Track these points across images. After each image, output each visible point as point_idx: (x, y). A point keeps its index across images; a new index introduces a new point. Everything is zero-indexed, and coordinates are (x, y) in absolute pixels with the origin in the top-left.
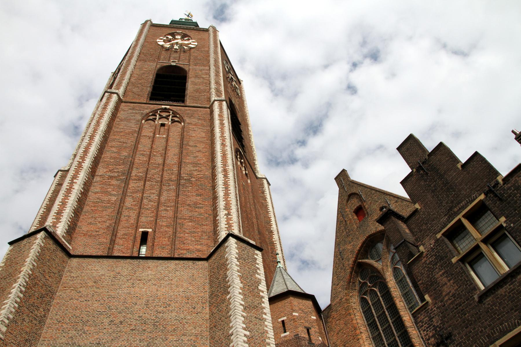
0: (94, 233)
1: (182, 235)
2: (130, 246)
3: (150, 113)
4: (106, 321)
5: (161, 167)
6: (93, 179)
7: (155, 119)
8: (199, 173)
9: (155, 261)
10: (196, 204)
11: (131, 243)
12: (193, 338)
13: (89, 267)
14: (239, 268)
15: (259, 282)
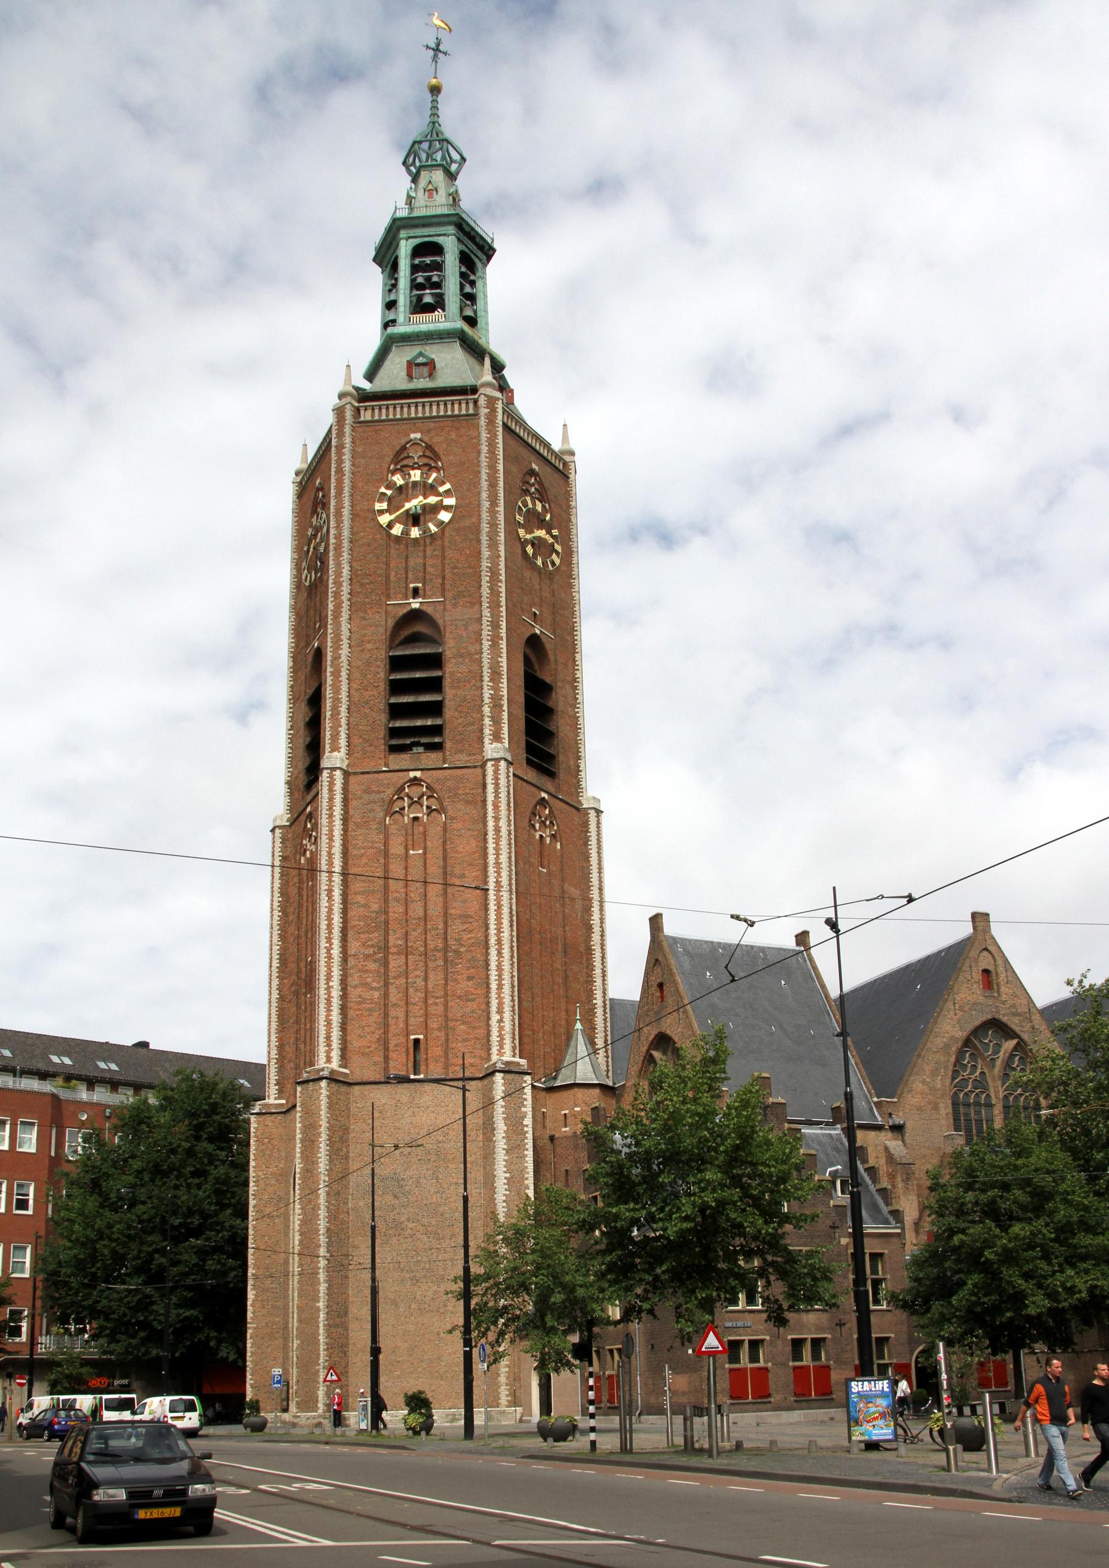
0: (367, 1050)
1: (454, 1045)
2: (404, 1061)
5: (422, 924)
7: (403, 808)
8: (469, 936)
10: (467, 993)
11: (404, 1055)
13: (371, 1095)
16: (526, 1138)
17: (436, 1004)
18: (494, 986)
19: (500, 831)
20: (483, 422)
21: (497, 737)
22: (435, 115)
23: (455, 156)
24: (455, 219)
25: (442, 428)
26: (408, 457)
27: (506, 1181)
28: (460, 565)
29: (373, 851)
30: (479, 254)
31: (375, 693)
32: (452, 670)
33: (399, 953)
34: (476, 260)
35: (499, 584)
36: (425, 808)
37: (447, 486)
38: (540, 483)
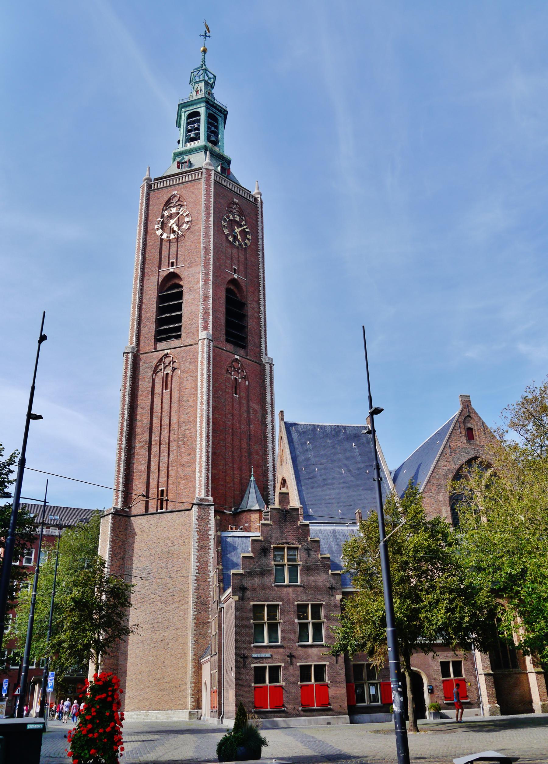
3: (157, 364)
4: (148, 554)
5: (168, 428)
6: (131, 452)
8: (189, 432)
9: (167, 514)
12: (183, 560)
13: (138, 522)
14: (197, 526)
15: (209, 529)
16: (210, 542)
17: (172, 470)
18: (198, 458)
19: (203, 375)
20: (203, 181)
21: (205, 328)
23: (211, 76)
24: (204, 99)
25: (186, 187)
26: (172, 203)
27: (197, 568)
28: (192, 248)
29: (146, 392)
30: (220, 114)
31: (152, 314)
32: (186, 298)
33: (156, 444)
34: (218, 117)
35: (210, 254)
36: (171, 368)
37: (188, 213)
38: (240, 208)
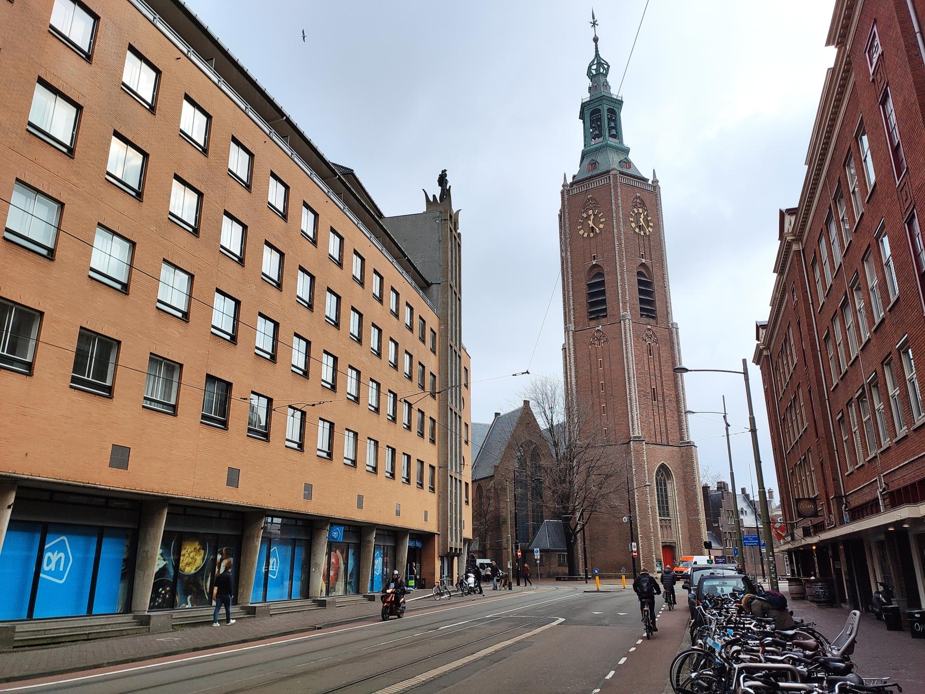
22: (597, 51)
